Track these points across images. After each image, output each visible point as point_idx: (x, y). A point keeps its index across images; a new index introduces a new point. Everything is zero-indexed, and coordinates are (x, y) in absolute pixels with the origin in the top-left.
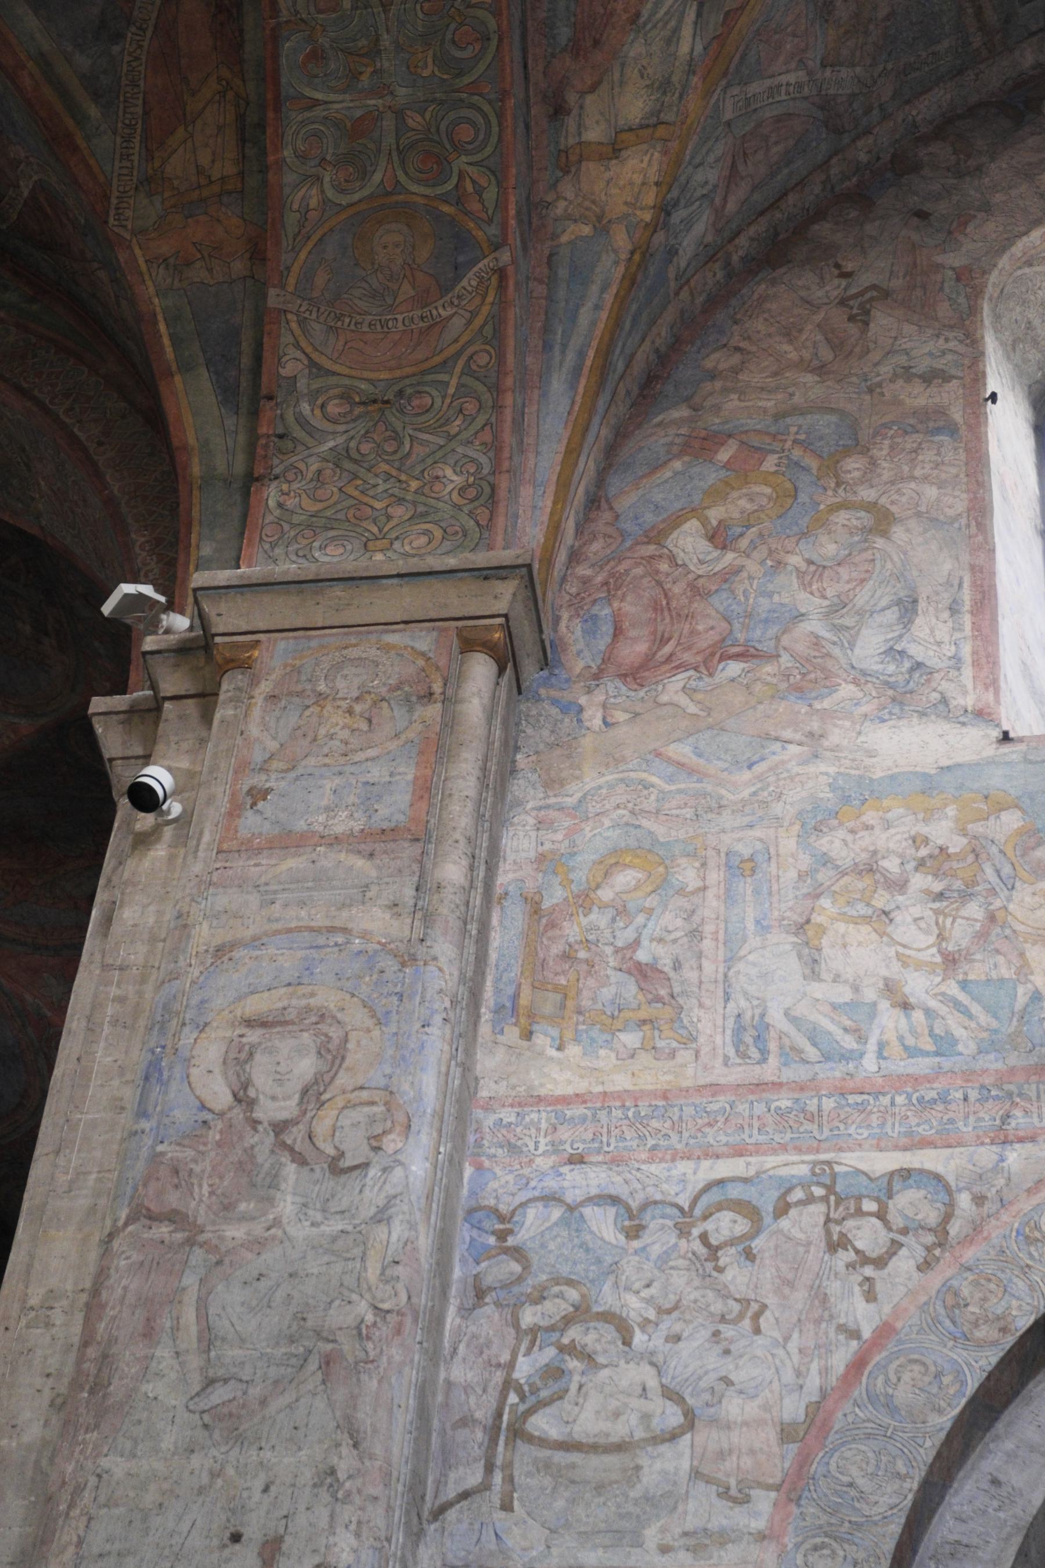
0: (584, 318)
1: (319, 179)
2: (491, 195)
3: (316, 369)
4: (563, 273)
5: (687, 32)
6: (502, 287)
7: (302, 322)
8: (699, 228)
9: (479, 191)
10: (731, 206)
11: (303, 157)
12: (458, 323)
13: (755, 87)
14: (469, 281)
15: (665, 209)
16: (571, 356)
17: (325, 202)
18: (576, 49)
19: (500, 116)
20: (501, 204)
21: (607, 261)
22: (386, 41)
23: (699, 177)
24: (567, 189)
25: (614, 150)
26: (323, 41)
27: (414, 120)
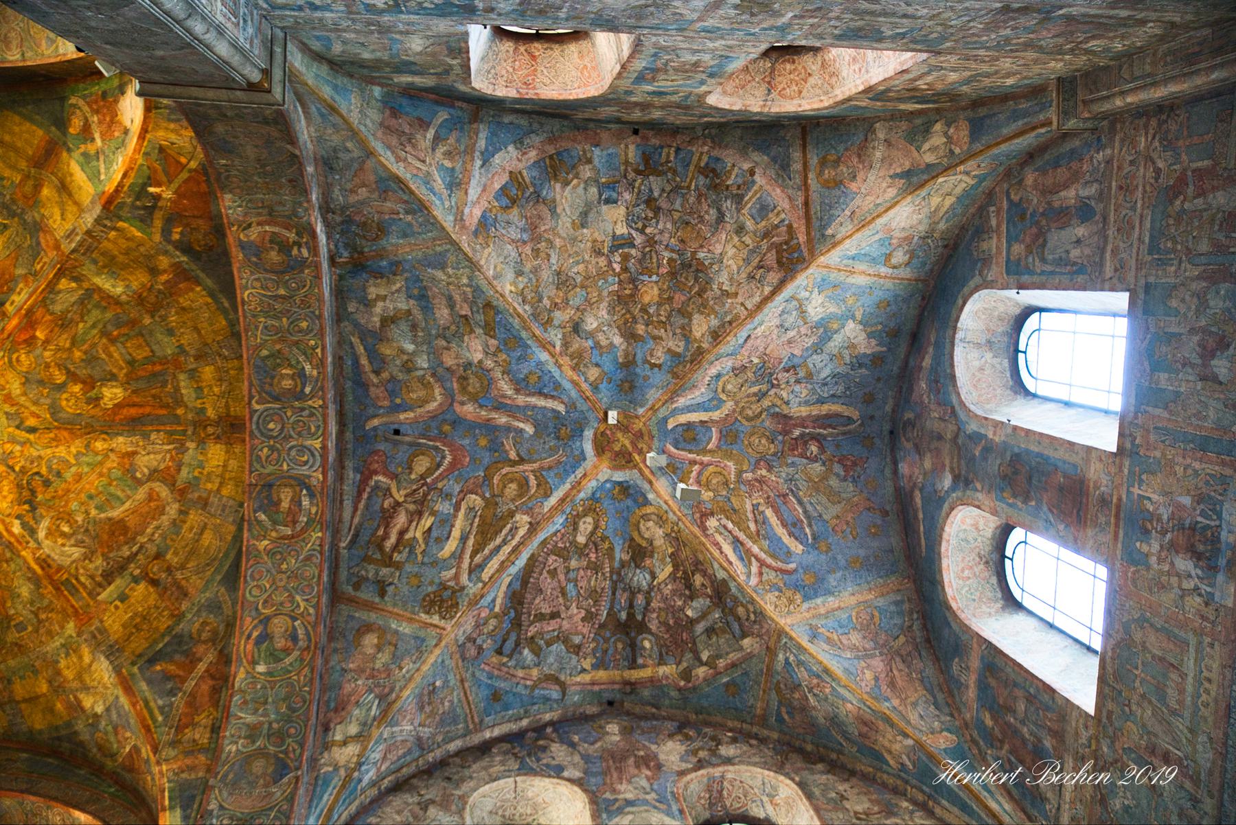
0: (325, 797)
1: (236, 743)
2: (298, 751)
3: (221, 807)
4: (320, 782)
5: (374, 708)
6: (297, 782)
7: (220, 791)
8: (371, 774)
9: (294, 750)
10: (383, 768)
11: (232, 736)
12: (279, 794)
13: (395, 729)
14: (285, 780)
15: (360, 764)
16: (318, 810)
17: (238, 750)
18: (336, 710)
19: (306, 726)
20: (301, 755)
21: (336, 779)
22: (270, 700)
23: (373, 756)
24: (326, 755)
25: (344, 743)
26: (248, 698)
27: (275, 726)
